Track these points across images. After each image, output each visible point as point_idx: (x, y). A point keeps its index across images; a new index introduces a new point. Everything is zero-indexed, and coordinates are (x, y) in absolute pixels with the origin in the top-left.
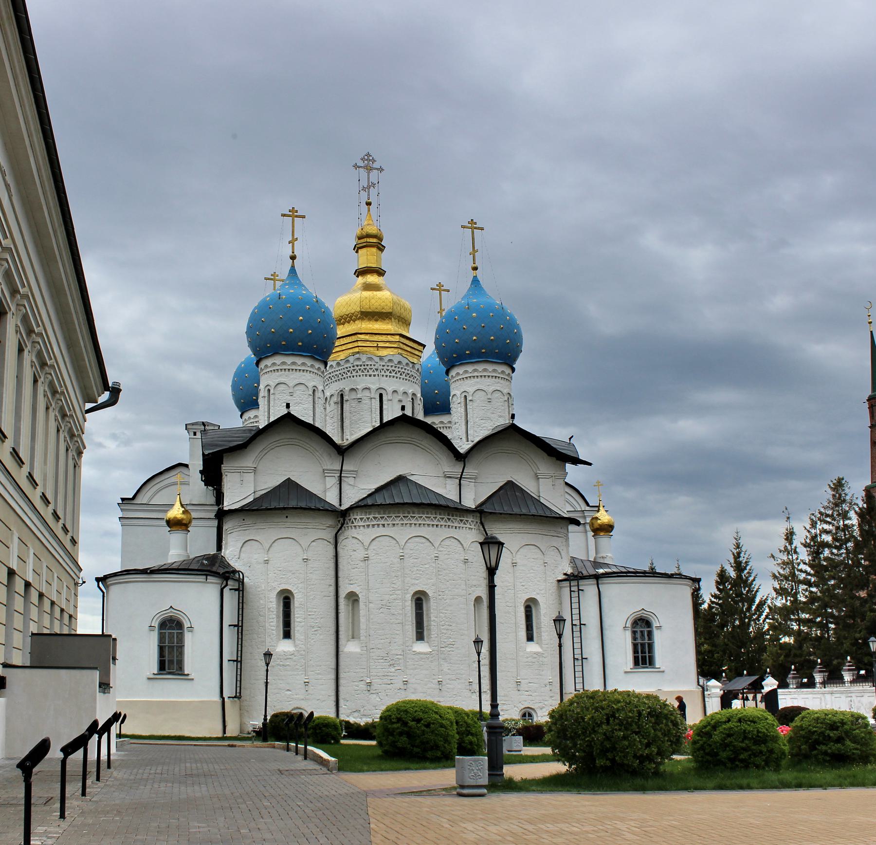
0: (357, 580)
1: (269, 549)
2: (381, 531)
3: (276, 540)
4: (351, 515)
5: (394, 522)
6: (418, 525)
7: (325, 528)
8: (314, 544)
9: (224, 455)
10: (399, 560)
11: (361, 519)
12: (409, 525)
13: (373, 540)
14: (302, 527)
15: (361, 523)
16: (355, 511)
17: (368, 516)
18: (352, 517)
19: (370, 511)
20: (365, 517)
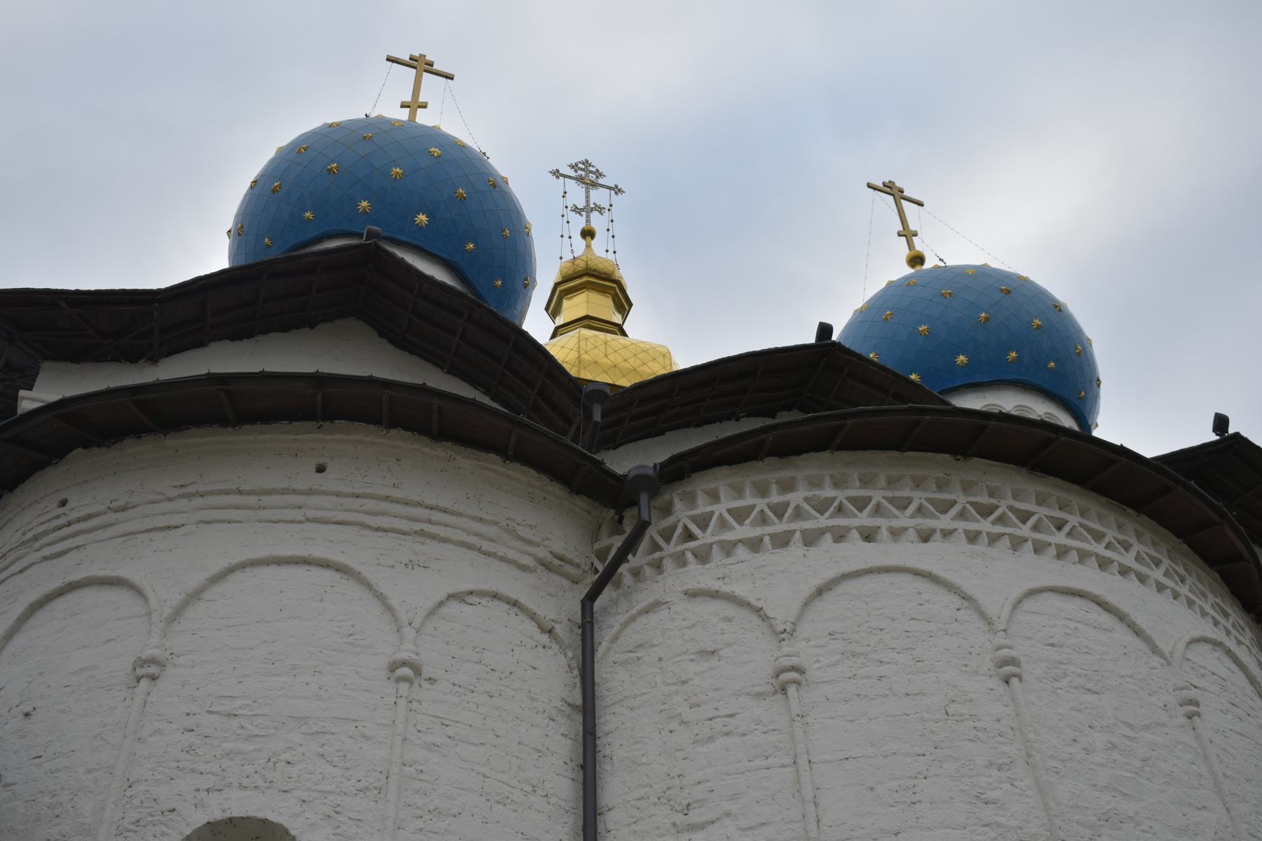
0: (733, 798)
1: (178, 613)
2: (856, 554)
3: (232, 570)
4: (678, 505)
5: (929, 523)
6: (1052, 551)
7: (526, 560)
8: (454, 608)
9: (46, 365)
10: (995, 683)
11: (740, 515)
12: (1006, 541)
13: (820, 592)
14: (405, 525)
15: (745, 531)
16: (701, 484)
17: (776, 498)
18: (682, 514)
19: (786, 474)
20: (761, 504)
